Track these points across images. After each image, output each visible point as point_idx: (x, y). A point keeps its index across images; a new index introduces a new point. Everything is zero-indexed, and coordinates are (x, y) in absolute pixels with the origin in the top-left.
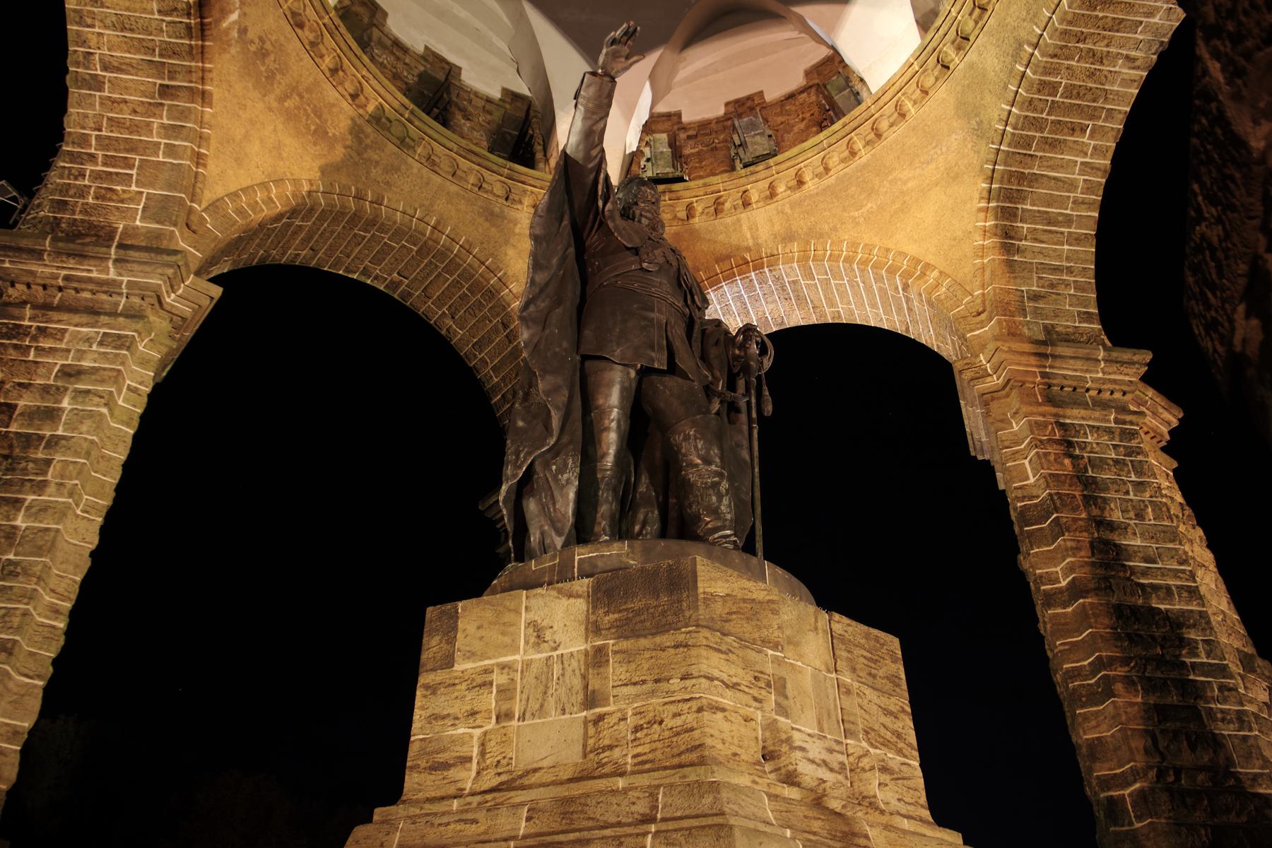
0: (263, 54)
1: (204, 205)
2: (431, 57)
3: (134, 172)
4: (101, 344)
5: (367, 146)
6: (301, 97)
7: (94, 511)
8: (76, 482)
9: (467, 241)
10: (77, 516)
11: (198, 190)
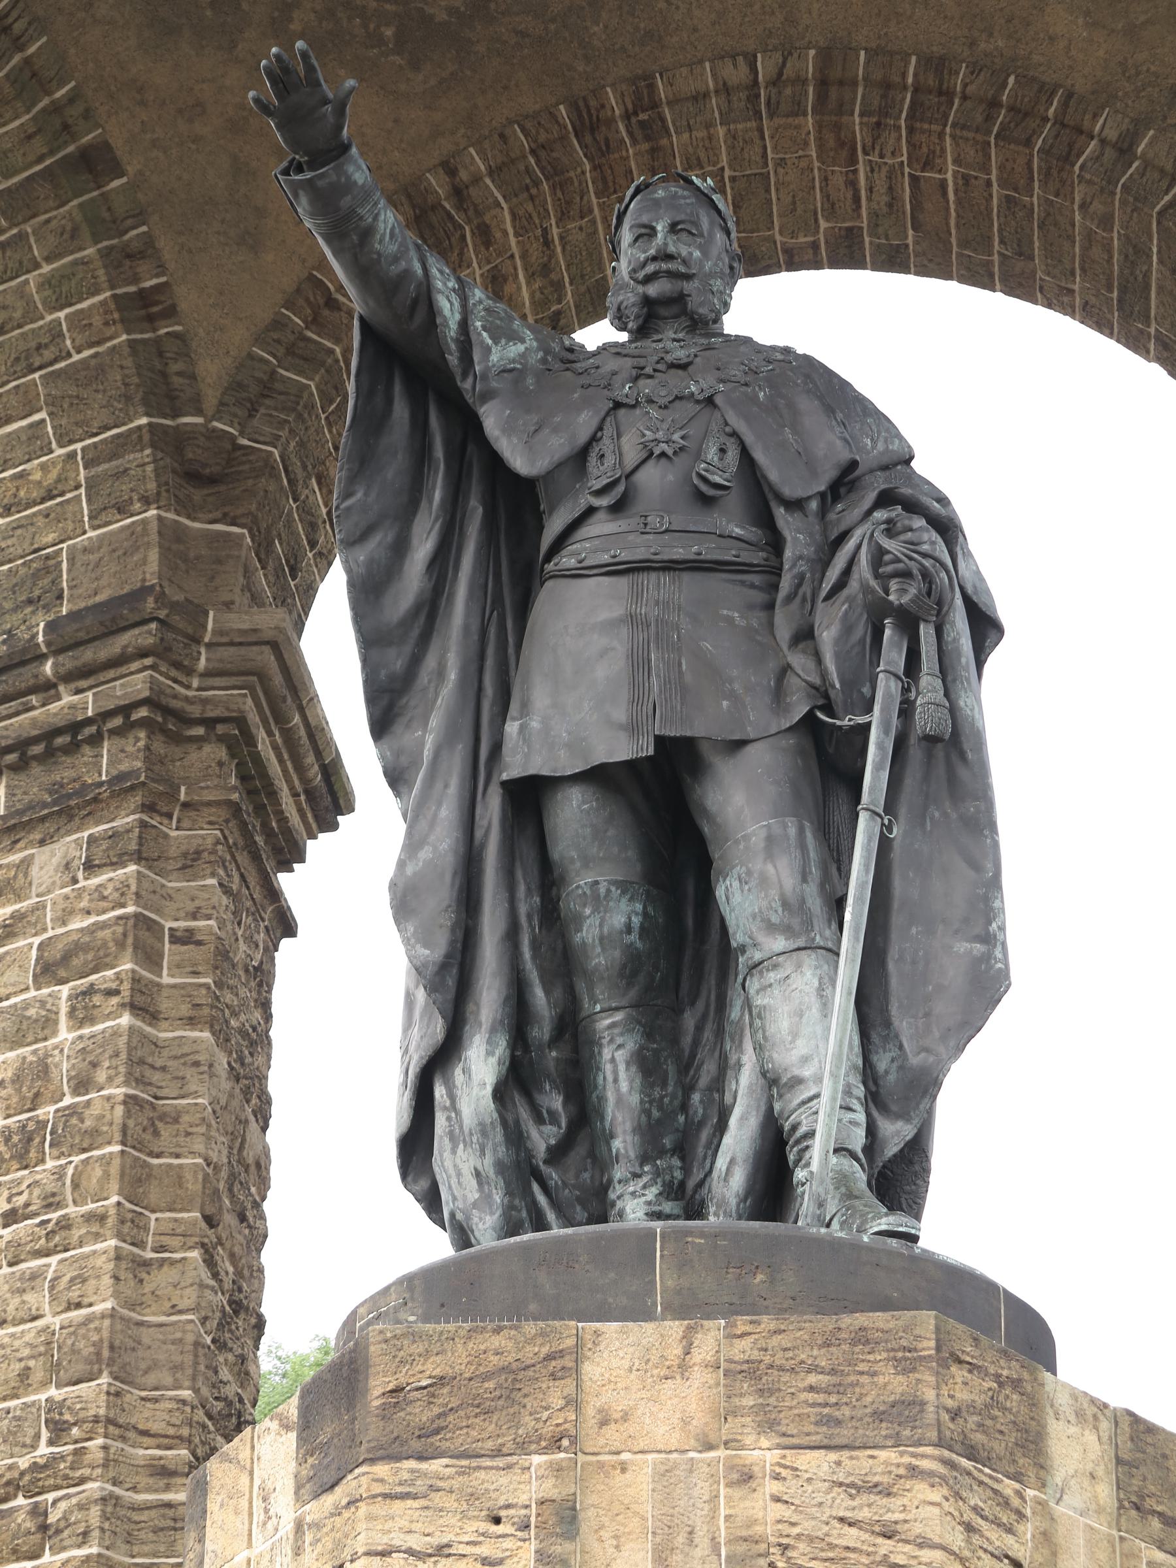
1: (211, 400)
3: (43, 415)
4: (90, 867)
7: (175, 1242)
11: (177, 381)
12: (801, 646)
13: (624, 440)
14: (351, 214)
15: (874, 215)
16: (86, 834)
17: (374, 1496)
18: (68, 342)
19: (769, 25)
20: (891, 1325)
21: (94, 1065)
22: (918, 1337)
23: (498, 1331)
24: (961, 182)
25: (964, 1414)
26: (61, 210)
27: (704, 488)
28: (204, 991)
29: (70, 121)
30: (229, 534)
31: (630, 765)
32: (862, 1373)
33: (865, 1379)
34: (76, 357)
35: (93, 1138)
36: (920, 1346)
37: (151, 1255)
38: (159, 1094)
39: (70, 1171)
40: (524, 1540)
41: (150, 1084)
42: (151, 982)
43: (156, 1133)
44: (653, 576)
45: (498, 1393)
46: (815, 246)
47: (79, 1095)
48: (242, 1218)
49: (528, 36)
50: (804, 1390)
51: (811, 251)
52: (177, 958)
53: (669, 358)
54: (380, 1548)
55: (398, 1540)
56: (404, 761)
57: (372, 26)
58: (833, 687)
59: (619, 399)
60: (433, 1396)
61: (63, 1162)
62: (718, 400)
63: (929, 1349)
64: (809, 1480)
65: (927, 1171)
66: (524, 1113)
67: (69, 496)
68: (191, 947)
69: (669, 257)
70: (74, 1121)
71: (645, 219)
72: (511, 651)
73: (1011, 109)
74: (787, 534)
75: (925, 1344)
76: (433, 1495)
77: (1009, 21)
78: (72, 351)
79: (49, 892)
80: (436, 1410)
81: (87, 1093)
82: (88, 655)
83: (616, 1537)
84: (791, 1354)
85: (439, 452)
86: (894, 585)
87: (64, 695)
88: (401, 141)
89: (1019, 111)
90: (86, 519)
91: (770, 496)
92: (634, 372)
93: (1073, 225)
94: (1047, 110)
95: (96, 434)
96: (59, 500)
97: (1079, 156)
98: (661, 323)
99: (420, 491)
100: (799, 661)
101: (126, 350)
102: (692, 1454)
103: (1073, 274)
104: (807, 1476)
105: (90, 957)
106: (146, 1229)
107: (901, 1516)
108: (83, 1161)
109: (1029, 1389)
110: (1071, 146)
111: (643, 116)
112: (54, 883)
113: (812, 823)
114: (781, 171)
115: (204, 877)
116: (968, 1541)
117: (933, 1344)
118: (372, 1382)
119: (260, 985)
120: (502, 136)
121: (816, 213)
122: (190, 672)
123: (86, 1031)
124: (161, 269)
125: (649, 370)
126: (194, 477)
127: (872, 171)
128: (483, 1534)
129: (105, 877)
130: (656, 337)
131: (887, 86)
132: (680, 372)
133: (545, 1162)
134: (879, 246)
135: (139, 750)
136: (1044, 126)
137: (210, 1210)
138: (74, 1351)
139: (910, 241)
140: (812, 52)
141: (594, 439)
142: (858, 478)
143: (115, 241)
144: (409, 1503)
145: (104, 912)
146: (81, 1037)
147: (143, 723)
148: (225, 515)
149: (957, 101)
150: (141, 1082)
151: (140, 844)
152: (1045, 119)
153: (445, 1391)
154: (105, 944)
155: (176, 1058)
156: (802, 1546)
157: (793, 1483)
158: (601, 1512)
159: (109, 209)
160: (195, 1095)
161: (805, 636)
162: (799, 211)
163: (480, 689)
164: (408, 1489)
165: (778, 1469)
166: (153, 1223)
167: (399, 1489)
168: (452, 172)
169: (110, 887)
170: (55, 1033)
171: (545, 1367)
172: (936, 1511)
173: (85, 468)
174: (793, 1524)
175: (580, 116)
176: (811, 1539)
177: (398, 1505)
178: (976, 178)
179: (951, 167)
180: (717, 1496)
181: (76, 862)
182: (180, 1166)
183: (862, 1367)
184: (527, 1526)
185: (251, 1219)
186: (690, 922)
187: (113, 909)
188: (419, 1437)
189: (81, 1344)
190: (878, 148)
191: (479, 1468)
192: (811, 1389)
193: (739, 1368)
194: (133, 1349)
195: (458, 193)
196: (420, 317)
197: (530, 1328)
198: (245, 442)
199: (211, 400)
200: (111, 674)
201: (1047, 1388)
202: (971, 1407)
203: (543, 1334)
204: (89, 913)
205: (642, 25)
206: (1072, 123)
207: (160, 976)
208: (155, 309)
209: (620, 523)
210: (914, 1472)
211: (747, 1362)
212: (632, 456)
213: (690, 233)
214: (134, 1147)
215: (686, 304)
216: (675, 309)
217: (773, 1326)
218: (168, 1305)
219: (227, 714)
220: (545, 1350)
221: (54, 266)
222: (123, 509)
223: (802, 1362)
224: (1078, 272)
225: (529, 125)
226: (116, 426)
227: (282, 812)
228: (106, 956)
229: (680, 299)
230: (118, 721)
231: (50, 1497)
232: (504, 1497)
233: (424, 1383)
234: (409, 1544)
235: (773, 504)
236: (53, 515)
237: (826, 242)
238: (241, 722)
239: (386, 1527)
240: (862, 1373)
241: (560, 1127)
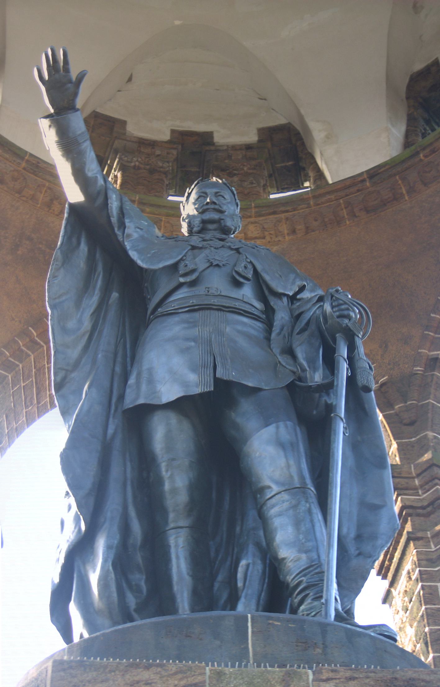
2: (181, 138)
23: (147, 667)
27: (238, 277)
31: (201, 395)
44: (212, 312)
57: (47, 258)
71: (203, 190)
85: (100, 268)
91: (267, 292)
100: (283, 359)
133: (135, 610)
163: (113, 371)
186: (214, 495)
217: (349, 674)
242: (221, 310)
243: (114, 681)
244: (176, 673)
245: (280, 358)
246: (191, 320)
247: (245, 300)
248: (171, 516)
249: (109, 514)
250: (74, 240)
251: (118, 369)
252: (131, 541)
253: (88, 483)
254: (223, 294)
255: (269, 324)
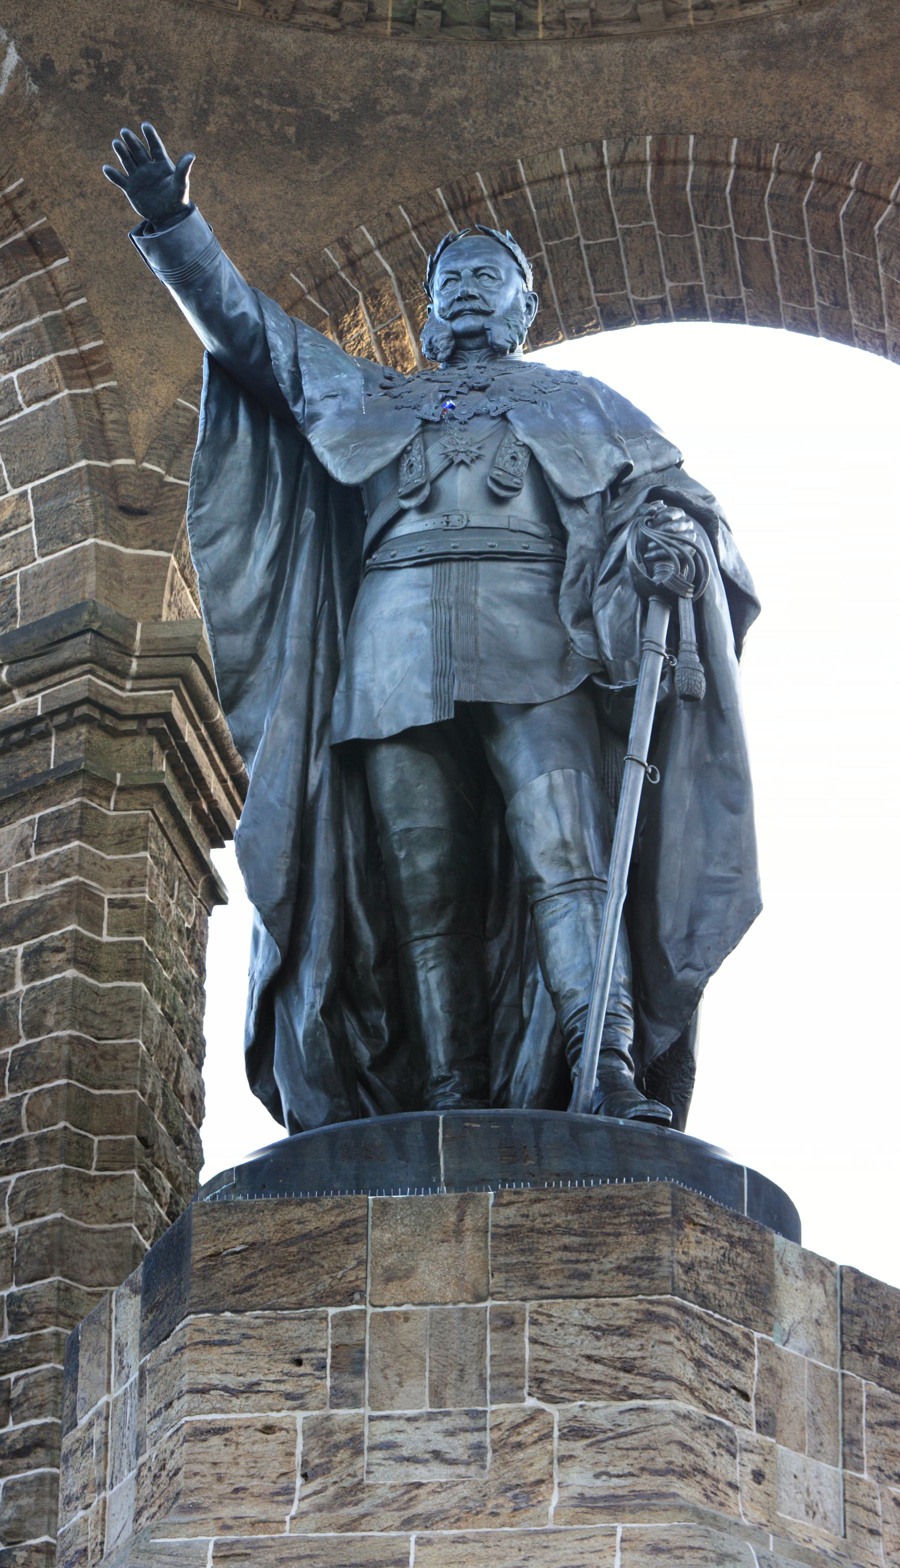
0: (107, 77)
1: (140, 448)
4: (41, 845)
5: (424, 85)
6: (231, 90)
8: (62, 1124)
9: (745, 144)
10: (93, 1180)
12: (582, 623)
13: (429, 451)
14: (197, 267)
15: (711, 275)
16: (37, 816)
17: (196, 1344)
18: (20, 398)
19: (612, 117)
20: (634, 1194)
21: (44, 1012)
22: (657, 1203)
23: (300, 1204)
24: (780, 243)
25: (697, 1268)
26: (13, 286)
28: (137, 948)
29: (19, 211)
30: (158, 558)
32: (609, 1234)
33: (611, 1240)
34: (27, 411)
35: (44, 1073)
36: (658, 1210)
37: (93, 1173)
38: (100, 1036)
39: (25, 1101)
40: (322, 1378)
41: (92, 1027)
42: (92, 940)
43: (98, 1068)
44: (454, 565)
45: (300, 1256)
46: (663, 303)
47: (32, 1037)
48: (178, 1141)
49: (410, 131)
50: (559, 1249)
51: (659, 307)
52: (114, 920)
53: (471, 383)
54: (200, 1387)
55: (215, 1379)
56: (250, 732)
57: (276, 127)
58: (607, 659)
59: (426, 417)
60: (246, 1259)
61: (20, 1094)
62: (510, 415)
63: (666, 1213)
64: (561, 1325)
65: (693, 1070)
66: (351, 1026)
67: (21, 529)
68: (127, 910)
69: (473, 297)
70: (28, 1060)
72: (340, 635)
73: (820, 180)
74: (570, 528)
75: (662, 1209)
76: (245, 1342)
77: (813, 107)
78: (24, 406)
79: (7, 866)
80: (248, 1271)
81: (39, 1035)
82: (37, 665)
83: (399, 1375)
84: (548, 1220)
86: (657, 567)
87: (17, 698)
88: (303, 222)
89: (826, 182)
90: (36, 548)
91: (556, 496)
92: (441, 396)
93: (878, 277)
94: (849, 180)
95: (44, 476)
96: (13, 533)
97: (877, 219)
98: (466, 353)
99: (261, 500)
100: (578, 636)
101: (68, 404)
102: (462, 1305)
103: (882, 319)
104: (560, 1321)
105: (41, 919)
106: (90, 1149)
107: (639, 1354)
108: (35, 1093)
109: (759, 1248)
110: (870, 210)
111: (508, 196)
112: (11, 858)
113: (589, 773)
114: (628, 239)
115: (137, 851)
116: (698, 1374)
117: (669, 1209)
118: (194, 1249)
119: (193, 944)
120: (388, 215)
121: (660, 275)
122: (124, 675)
123: (38, 983)
124: (99, 334)
125: (452, 393)
126: (128, 511)
127: (705, 236)
128: (286, 1374)
129: (53, 852)
130: (462, 365)
131: (713, 163)
132: (480, 394)
133: (370, 1068)
134: (717, 301)
135: (80, 743)
136: (847, 194)
137: (144, 1133)
138: (30, 1254)
139: (743, 295)
140: (649, 138)
141: (405, 451)
142: (634, 480)
143: (59, 311)
144: (226, 1349)
145: (52, 881)
146: (33, 988)
147: (86, 719)
148: (154, 542)
149: (773, 175)
150: (83, 1025)
151: (81, 823)
152: (848, 188)
153: (255, 1255)
154: (52, 908)
155: (114, 1004)
156: (555, 1380)
157: (549, 1328)
158: (386, 1354)
159: (53, 285)
160: (131, 1035)
161: (585, 616)
162: (647, 273)
163: (313, 669)
164: (225, 1338)
165: (536, 1316)
166: (96, 1145)
167: (216, 1338)
168: (347, 247)
169: (57, 859)
170: (12, 985)
171: (340, 1234)
172: (668, 1348)
173: (35, 505)
174: (548, 1362)
175: (454, 197)
176: (562, 1373)
177: (216, 1350)
178: (793, 240)
179: (771, 232)
180: (485, 1340)
181: (30, 840)
182: (118, 1096)
183: (609, 1229)
184: (324, 1367)
185: (187, 1142)
187: (59, 879)
188: (234, 1293)
189: (35, 1249)
190: (708, 218)
191: (284, 1318)
192: (565, 1248)
193: (504, 1231)
194: (80, 1252)
195: (352, 263)
196: (256, 353)
197: (328, 1202)
198: (171, 479)
199: (140, 448)
200: (56, 678)
201: (776, 1248)
202: (704, 1262)
203: (338, 1206)
204: (39, 883)
205: (505, 120)
206: (871, 190)
207: (100, 935)
208: (93, 368)
209: (427, 522)
210: (650, 1317)
211: (512, 1226)
212: (436, 464)
213: (490, 276)
214: (78, 1081)
215: (486, 337)
216: (478, 341)
217: (534, 1195)
218: (109, 1214)
219: (155, 711)
220: (340, 1219)
221: (8, 333)
222: (66, 540)
223: (558, 1226)
224: (886, 318)
225: (411, 205)
226: (58, 469)
227: (211, 796)
228: (54, 919)
229: (482, 332)
230: (62, 718)
231: (12, 1376)
232: (306, 1343)
233: (238, 1249)
234: (224, 1383)
235: (558, 502)
236: (8, 546)
237: (672, 299)
238: (168, 717)
239: (206, 1369)
240: (609, 1234)
241: (383, 1039)
242: (468, 560)
243: (262, 1222)
244: (332, 1209)
245: (573, 632)
246: (422, 583)
247: (512, 527)
248: (414, 920)
249: (314, 932)
250: (226, 422)
251: (321, 666)
252: (360, 960)
253: (279, 885)
254: (472, 524)
255: (558, 560)
